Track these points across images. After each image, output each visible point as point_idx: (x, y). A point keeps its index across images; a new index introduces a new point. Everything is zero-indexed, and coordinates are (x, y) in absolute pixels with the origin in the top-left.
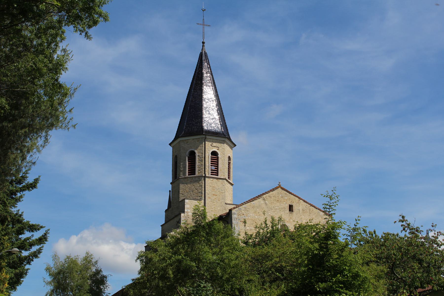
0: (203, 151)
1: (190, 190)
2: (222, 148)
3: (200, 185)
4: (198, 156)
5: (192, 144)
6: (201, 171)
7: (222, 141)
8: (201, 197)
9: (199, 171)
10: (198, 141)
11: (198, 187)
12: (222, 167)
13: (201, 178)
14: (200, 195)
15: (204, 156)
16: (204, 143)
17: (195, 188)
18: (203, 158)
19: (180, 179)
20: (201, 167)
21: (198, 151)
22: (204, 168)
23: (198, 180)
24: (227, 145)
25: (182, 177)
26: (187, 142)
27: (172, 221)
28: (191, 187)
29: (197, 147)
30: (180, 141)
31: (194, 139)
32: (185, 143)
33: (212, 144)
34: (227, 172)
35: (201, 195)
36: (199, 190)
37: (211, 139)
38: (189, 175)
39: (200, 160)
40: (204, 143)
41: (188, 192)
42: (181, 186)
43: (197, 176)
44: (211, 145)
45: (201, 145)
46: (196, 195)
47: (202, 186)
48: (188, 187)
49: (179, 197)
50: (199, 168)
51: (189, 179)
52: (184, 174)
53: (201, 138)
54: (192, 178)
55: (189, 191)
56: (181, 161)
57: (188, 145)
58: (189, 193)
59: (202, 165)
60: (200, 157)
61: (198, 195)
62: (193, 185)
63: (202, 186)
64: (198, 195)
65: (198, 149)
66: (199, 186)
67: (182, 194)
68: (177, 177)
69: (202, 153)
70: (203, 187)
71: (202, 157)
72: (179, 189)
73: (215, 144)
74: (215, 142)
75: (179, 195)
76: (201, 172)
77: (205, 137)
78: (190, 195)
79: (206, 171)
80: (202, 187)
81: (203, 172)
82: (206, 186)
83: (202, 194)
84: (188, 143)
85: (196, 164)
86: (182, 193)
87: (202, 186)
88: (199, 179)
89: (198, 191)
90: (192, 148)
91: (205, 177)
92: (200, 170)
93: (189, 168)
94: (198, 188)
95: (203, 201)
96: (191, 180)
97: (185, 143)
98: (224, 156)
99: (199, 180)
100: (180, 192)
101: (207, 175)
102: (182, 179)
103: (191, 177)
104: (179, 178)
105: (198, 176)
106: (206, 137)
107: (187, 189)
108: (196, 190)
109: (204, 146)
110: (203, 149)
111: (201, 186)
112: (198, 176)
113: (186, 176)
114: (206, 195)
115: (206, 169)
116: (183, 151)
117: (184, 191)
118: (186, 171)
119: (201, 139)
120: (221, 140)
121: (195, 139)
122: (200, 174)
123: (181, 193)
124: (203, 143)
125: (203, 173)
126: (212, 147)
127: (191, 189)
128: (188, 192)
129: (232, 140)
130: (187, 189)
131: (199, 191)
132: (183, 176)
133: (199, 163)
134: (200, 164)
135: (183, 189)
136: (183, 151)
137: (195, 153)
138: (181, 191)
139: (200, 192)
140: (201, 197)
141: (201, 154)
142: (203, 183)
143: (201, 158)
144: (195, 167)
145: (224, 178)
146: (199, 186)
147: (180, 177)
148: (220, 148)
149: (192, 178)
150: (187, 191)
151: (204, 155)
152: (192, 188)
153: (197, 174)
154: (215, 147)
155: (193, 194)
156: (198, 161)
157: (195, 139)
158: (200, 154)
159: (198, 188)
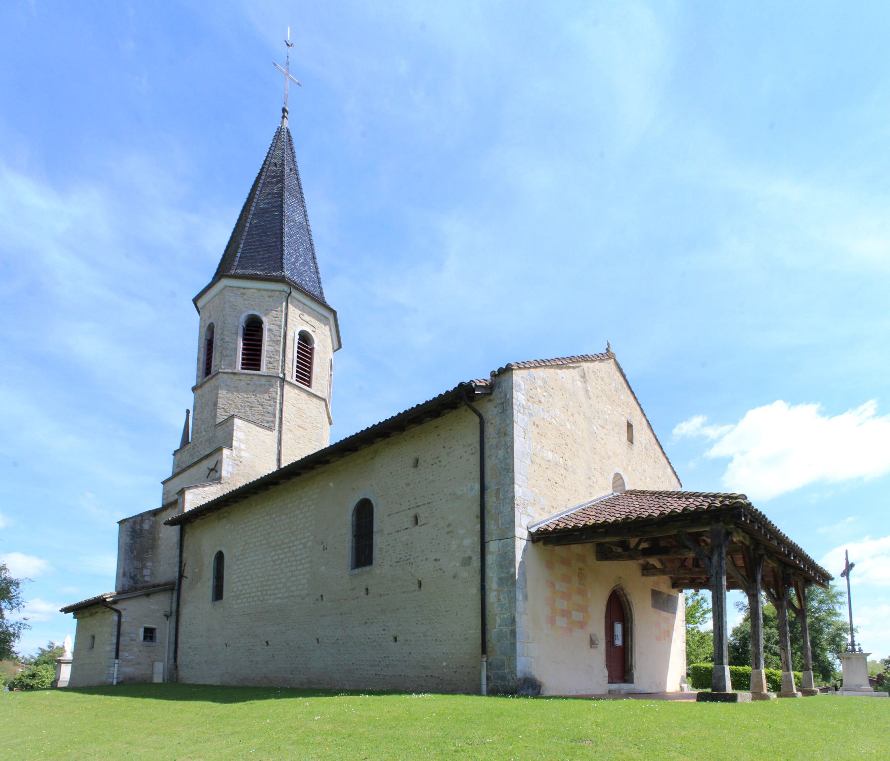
0: (281, 321)
1: (244, 404)
3: (269, 397)
4: (270, 330)
5: (255, 301)
6: (275, 365)
8: (272, 424)
9: (271, 366)
10: (269, 297)
11: (266, 400)
13: (273, 380)
14: (269, 419)
15: (283, 334)
16: (284, 304)
17: (258, 401)
18: (280, 336)
19: (220, 375)
20: (276, 357)
21: (269, 320)
22: (281, 360)
23: (265, 385)
25: (226, 371)
26: (243, 294)
27: (193, 470)
28: (247, 398)
29: (267, 310)
30: (224, 289)
31: (260, 290)
32: (236, 294)
35: (272, 419)
36: (267, 408)
38: (242, 369)
39: (274, 341)
41: (239, 406)
42: (222, 393)
43: (263, 374)
45: (279, 309)
46: (260, 417)
47: (275, 400)
48: (240, 397)
49: (215, 417)
50: (271, 358)
51: (243, 377)
52: (233, 364)
53: (280, 291)
54: (253, 378)
55: (241, 406)
56: (224, 333)
57: (246, 300)
58: (243, 411)
59: (278, 351)
60: (273, 334)
61: (265, 418)
62: (254, 395)
63: (274, 399)
64: (265, 418)
65: (270, 314)
66: (268, 398)
67: (223, 410)
68: (212, 372)
69: (280, 326)
70: (278, 401)
71: (279, 334)
72: (217, 398)
75: (216, 412)
76: (274, 366)
77: (289, 291)
78: (243, 414)
79: (286, 368)
80: (276, 402)
81: (280, 369)
82: (284, 403)
83: (275, 417)
84: (245, 297)
85: (263, 348)
86: (223, 408)
87: (275, 400)
88: (268, 383)
89: (265, 410)
90: (254, 310)
91: (283, 380)
92: (272, 363)
93: (243, 354)
94: (265, 401)
95: (276, 433)
96: (249, 382)
97: (236, 294)
99: (269, 385)
100: (219, 405)
101: (288, 378)
102: (225, 376)
103: (250, 374)
104: (219, 373)
105: (266, 374)
106: (290, 292)
107: (238, 402)
108: (259, 406)
109: (284, 310)
110: (282, 318)
111: (274, 398)
112: (268, 376)
113: (235, 368)
114: (284, 421)
115: (286, 365)
116: (230, 311)
117: (230, 404)
118: (237, 358)
119: (278, 293)
121: (264, 290)
122: (272, 372)
123: (222, 406)
124: (282, 303)
125: (280, 372)
127: (247, 401)
128: (239, 406)
130: (238, 402)
131: (269, 410)
132: (228, 369)
133: (270, 347)
134: (274, 350)
135: (226, 399)
136: (230, 311)
137: (261, 323)
138: (220, 401)
139: (268, 413)
140: (272, 424)
141: (277, 328)
142: (279, 393)
143: (275, 336)
144: (260, 355)
146: (268, 398)
147: (220, 370)
149: (251, 377)
150: (236, 406)
151: (283, 331)
152: (249, 400)
153: (264, 369)
155: (253, 415)
156: (268, 341)
157: (262, 291)
158: (272, 327)
159: (265, 401)
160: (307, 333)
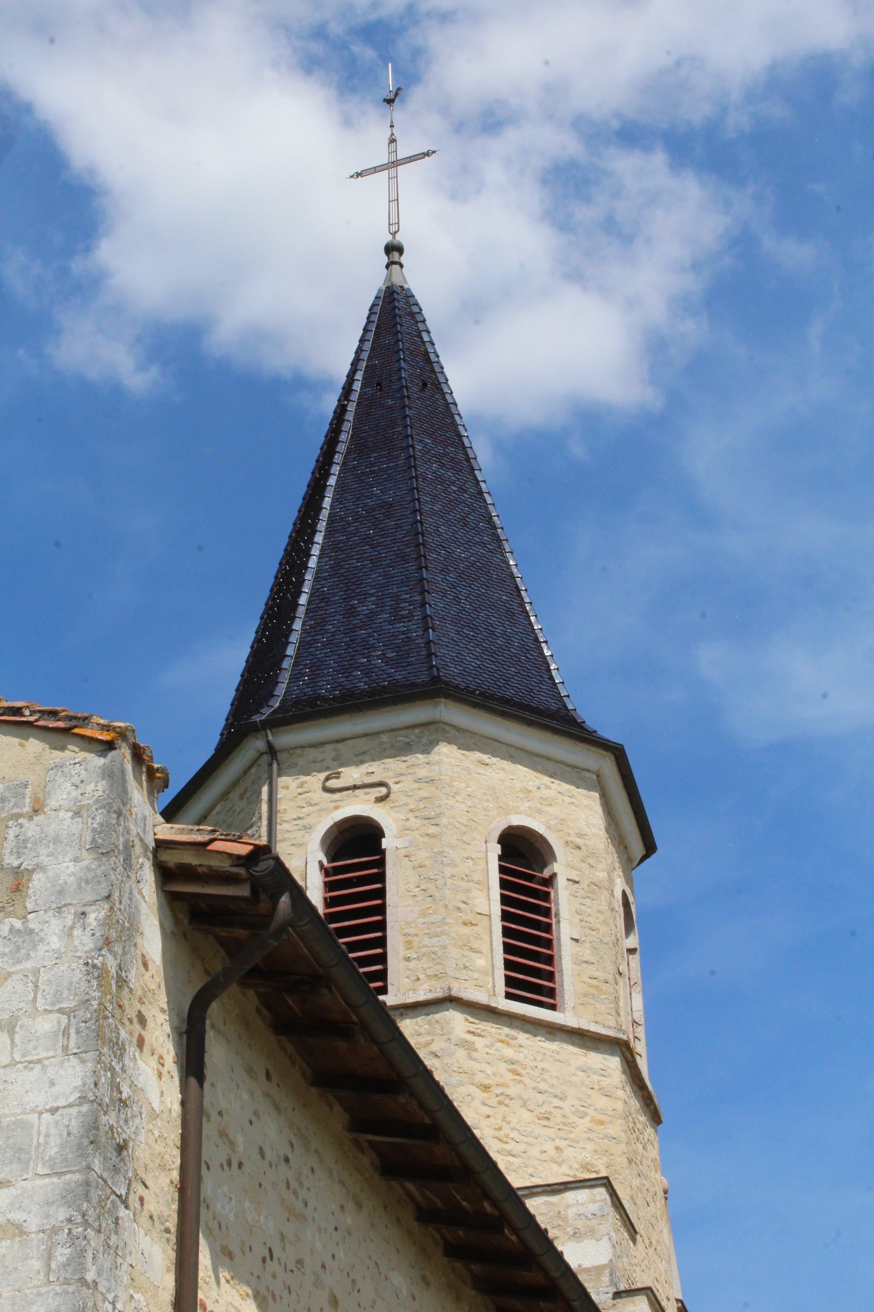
2: (418, 780)
7: (417, 731)
12: (423, 914)
16: (265, 789)
24: (477, 755)
31: (225, 795)
33: (337, 775)
34: (485, 948)
37: (329, 747)
40: (265, 789)
44: (326, 789)
73: (352, 774)
74: (359, 759)
98: (432, 830)
120: (407, 728)
126: (337, 796)
129: (591, 723)
145: (439, 994)
148: (394, 788)
154: (355, 787)
160: (328, 842)
